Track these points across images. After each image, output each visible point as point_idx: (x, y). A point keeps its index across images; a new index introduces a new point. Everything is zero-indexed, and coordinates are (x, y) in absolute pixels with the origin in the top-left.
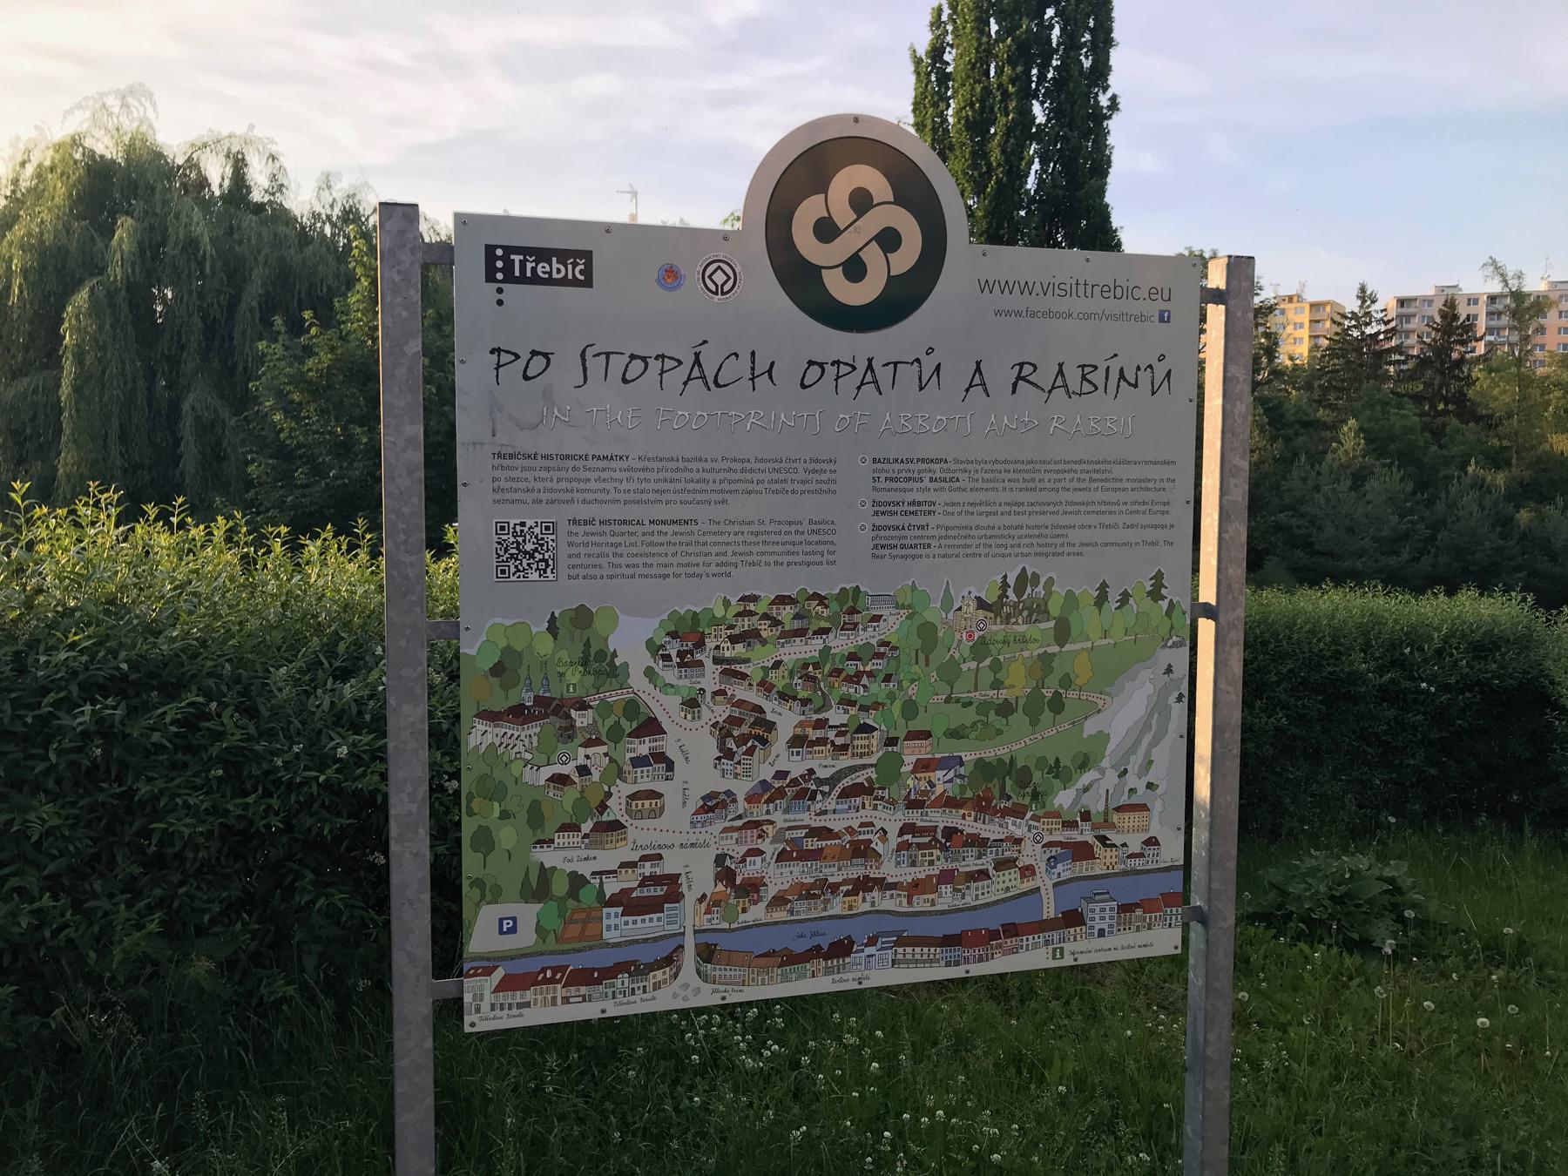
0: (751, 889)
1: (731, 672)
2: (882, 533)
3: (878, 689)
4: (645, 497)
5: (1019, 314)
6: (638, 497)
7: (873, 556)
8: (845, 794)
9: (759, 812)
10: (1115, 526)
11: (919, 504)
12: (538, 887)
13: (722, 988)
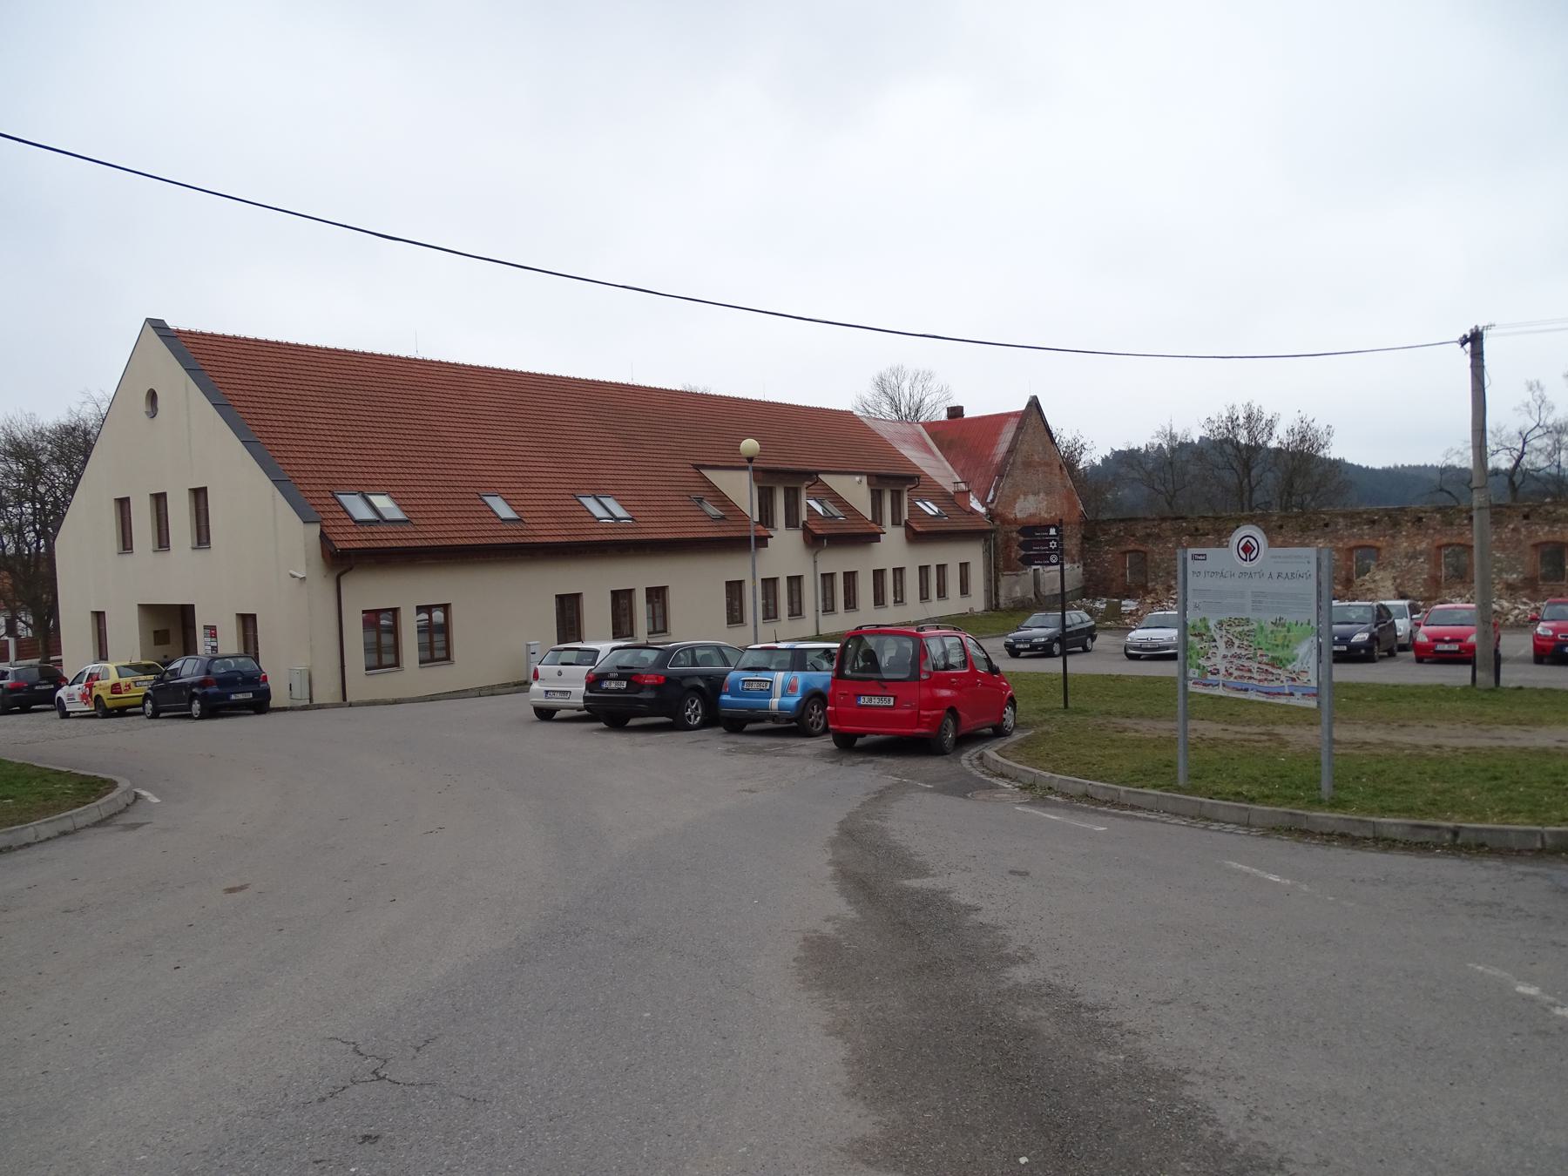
12: (1198, 667)
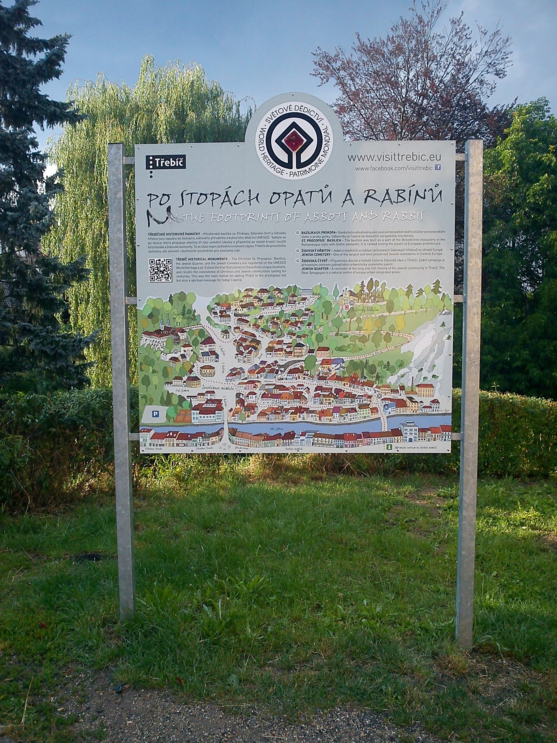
0: (251, 408)
1: (242, 320)
2: (306, 263)
3: (305, 329)
4: (206, 249)
5: (367, 169)
6: (203, 249)
7: (303, 273)
8: (290, 372)
9: (254, 377)
10: (416, 260)
11: (323, 251)
12: (167, 400)
13: (239, 447)
